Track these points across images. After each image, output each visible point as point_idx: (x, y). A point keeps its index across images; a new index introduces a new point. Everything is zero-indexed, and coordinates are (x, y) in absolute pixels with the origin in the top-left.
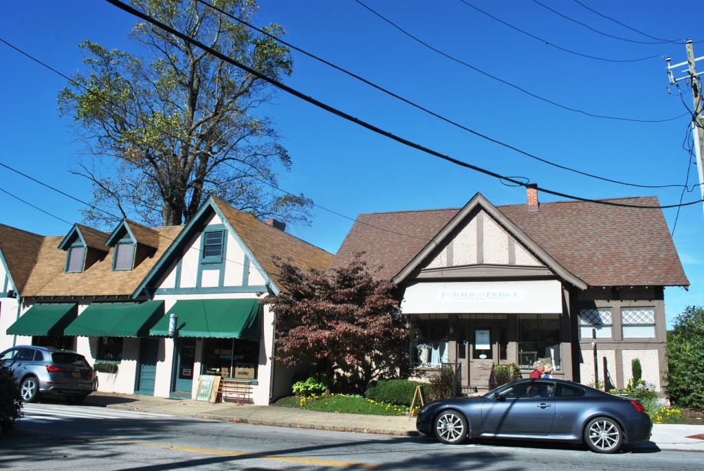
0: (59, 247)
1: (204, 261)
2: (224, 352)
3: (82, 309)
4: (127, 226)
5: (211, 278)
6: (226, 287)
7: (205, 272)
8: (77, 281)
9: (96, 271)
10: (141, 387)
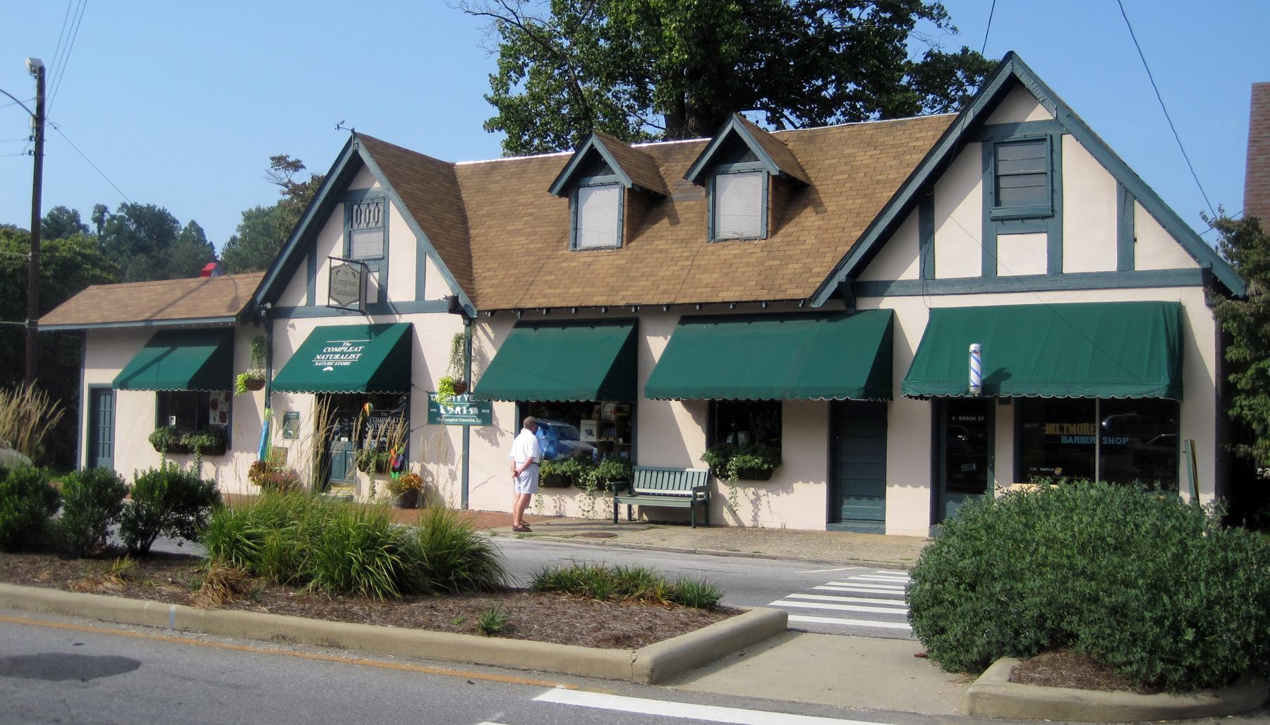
0: (550, 190)
1: (998, 212)
2: (1073, 428)
3: (656, 345)
4: (364, 155)
5: (1023, 254)
6: (1007, 280)
7: (1003, 241)
8: (621, 269)
9: (661, 244)
10: (845, 514)
